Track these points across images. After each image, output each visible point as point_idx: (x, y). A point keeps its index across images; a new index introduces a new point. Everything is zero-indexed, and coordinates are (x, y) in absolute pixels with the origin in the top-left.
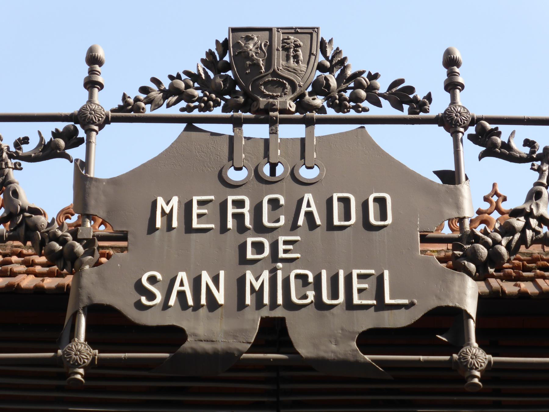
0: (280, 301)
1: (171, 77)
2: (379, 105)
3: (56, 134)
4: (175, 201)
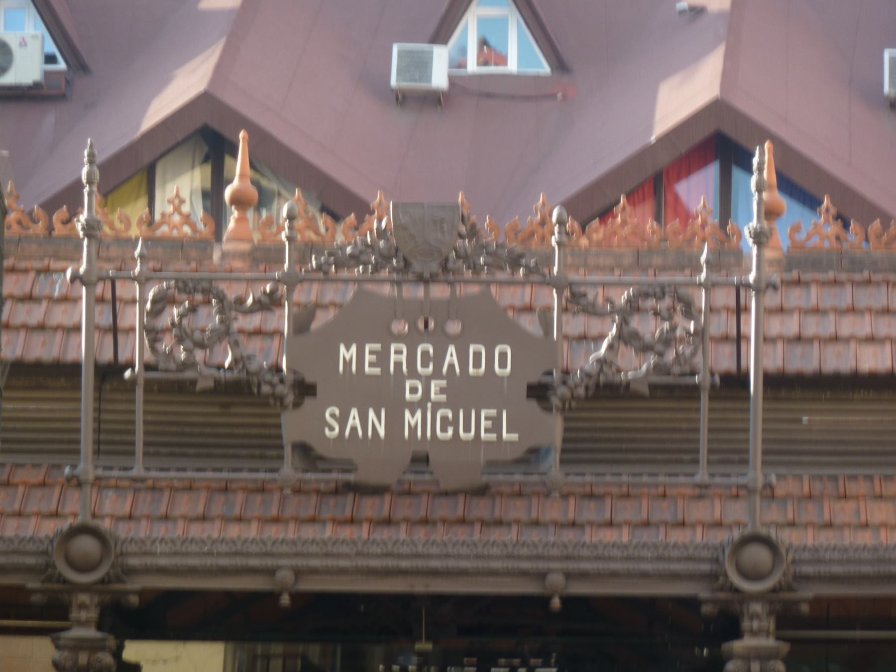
4: (354, 349)
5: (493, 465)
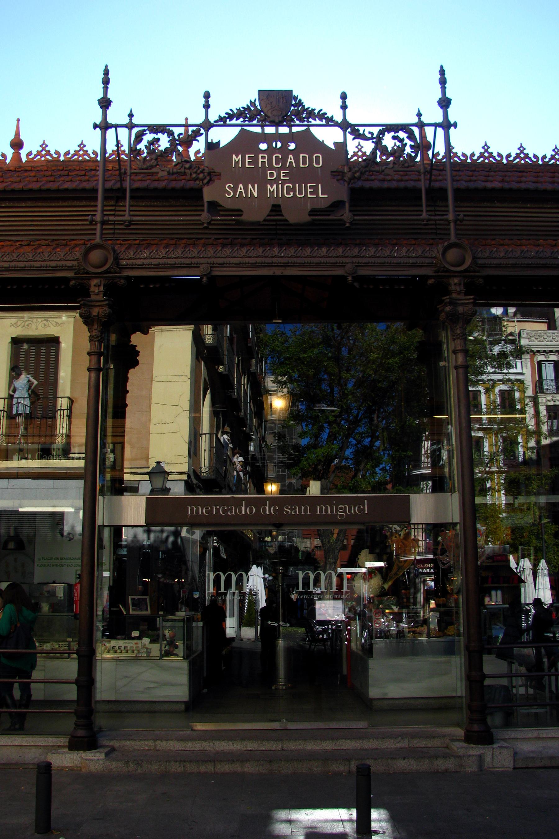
0: (280, 196)
1: (237, 109)
2: (315, 120)
3: (193, 131)
4: (240, 156)
5: (313, 212)
